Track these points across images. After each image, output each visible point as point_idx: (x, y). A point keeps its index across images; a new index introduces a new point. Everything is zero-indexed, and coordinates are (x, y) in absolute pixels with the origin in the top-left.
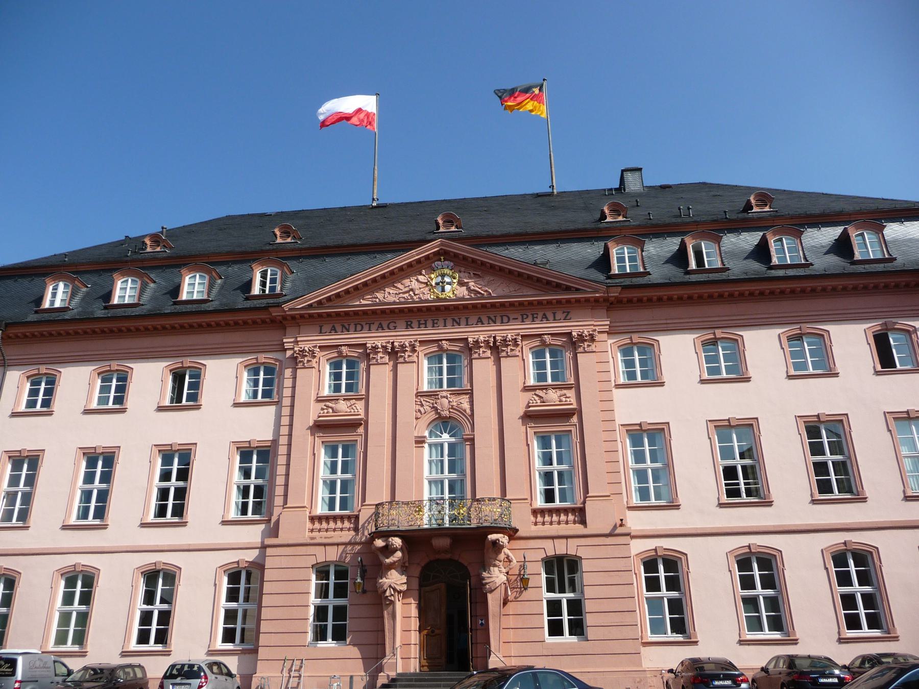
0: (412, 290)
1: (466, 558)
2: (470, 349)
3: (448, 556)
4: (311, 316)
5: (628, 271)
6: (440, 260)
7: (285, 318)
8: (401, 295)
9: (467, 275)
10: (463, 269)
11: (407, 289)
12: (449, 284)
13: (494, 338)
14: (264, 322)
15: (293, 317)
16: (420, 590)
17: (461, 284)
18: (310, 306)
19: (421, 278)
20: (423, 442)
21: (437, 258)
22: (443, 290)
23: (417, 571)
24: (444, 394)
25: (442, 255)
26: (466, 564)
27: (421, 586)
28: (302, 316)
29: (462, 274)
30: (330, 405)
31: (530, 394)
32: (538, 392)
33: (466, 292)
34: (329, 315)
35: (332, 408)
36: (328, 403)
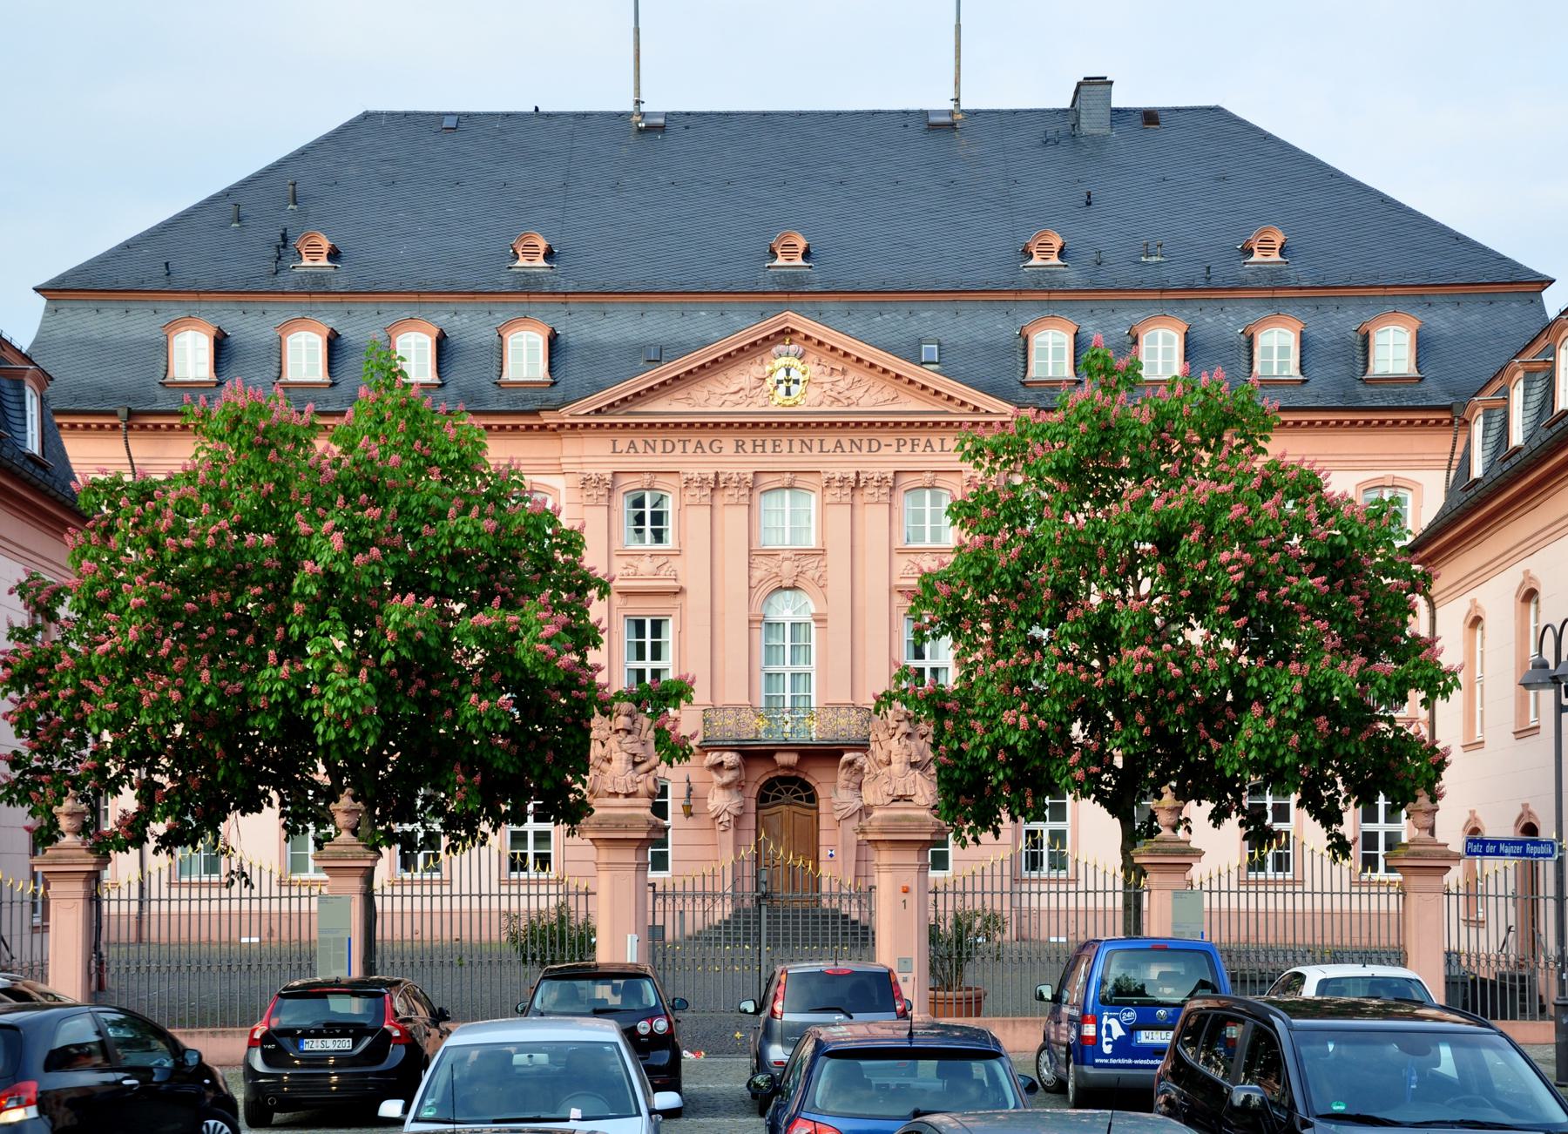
4: (600, 425)
12: (796, 382)
14: (529, 427)
15: (574, 426)
18: (598, 411)
22: (788, 393)
28: (587, 425)
34: (626, 425)
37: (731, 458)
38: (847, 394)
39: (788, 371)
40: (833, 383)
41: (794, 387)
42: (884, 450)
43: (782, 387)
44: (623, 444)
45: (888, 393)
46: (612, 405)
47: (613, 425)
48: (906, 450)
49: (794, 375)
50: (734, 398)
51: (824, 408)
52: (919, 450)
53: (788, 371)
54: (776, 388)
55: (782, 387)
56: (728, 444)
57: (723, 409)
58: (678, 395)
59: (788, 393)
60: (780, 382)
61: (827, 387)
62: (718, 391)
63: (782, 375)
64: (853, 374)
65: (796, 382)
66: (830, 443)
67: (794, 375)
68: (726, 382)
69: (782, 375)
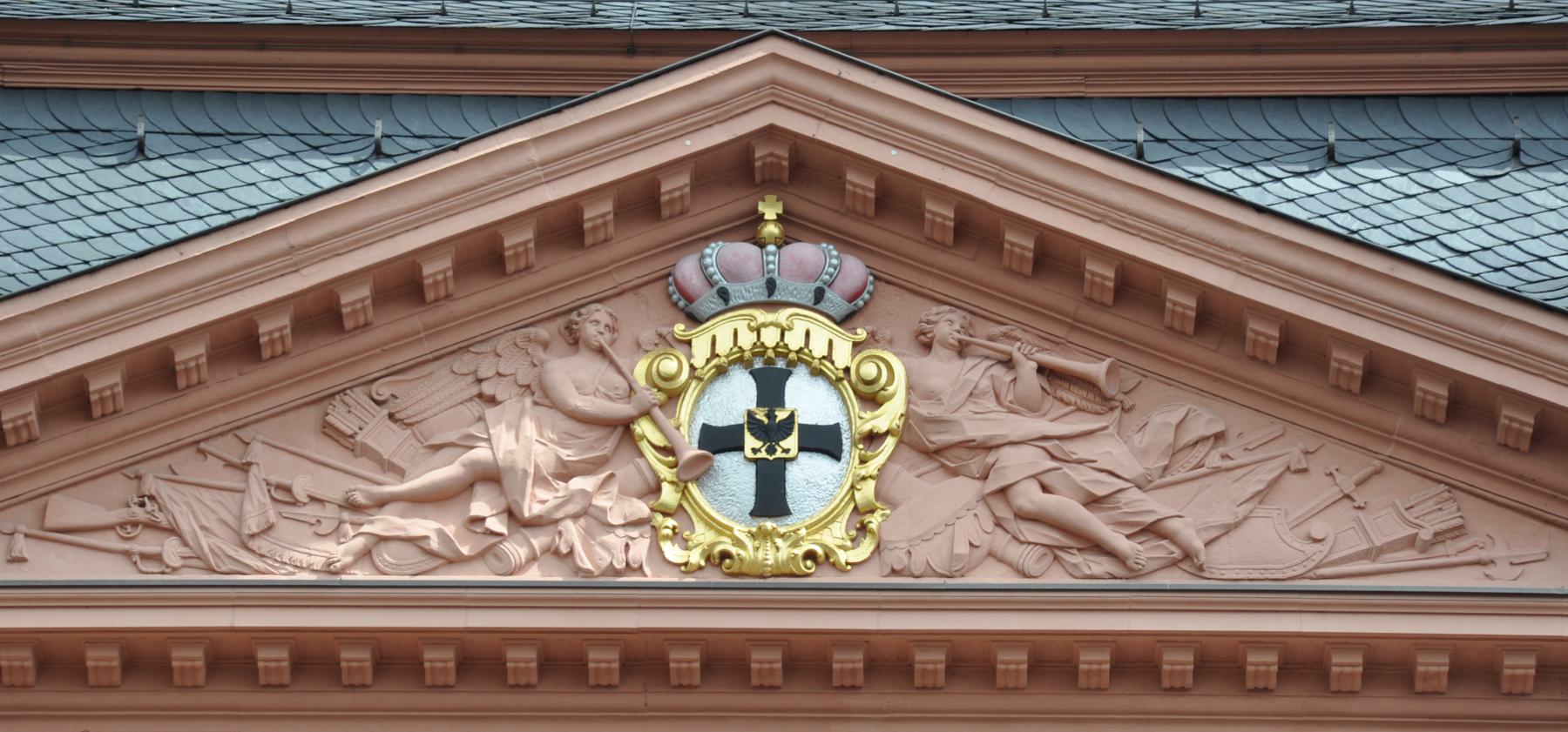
0: (490, 477)
6: (748, 227)
8: (386, 523)
9: (976, 372)
10: (948, 325)
11: (446, 471)
12: (823, 441)
17: (928, 445)
19: (578, 380)
21: (728, 204)
22: (771, 499)
25: (771, 184)
29: (942, 371)
33: (973, 528)
38: (1153, 506)
39: (771, 386)
41: (810, 477)
49: (809, 401)
53: (771, 386)
54: (695, 472)
55: (736, 475)
58: (69, 510)
59: (771, 499)
60: (720, 440)
61: (1017, 464)
62: (335, 487)
63: (736, 398)
64: (1169, 414)
65: (823, 441)
67: (809, 401)
68: (384, 438)
69: (736, 398)
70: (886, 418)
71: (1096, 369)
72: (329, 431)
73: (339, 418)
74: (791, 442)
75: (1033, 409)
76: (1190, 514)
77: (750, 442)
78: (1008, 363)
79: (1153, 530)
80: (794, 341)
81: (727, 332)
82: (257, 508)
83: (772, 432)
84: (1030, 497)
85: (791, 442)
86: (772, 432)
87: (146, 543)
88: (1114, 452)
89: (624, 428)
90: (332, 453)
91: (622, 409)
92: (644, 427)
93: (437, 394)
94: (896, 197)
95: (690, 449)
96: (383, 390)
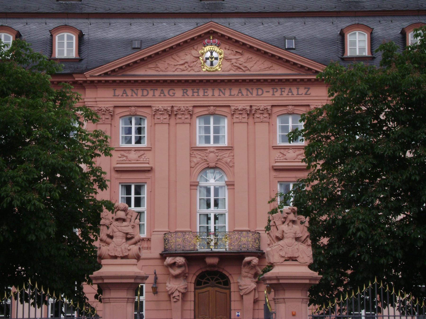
1: (229, 271)
2: (233, 115)
3: (216, 269)
4: (107, 81)
5: (358, 54)
7: (85, 82)
9: (229, 52)
13: (251, 106)
15: (92, 82)
16: (194, 292)
18: (106, 74)
19: (194, 52)
20: (197, 186)
22: (212, 64)
23: (192, 279)
24: (212, 150)
26: (227, 275)
27: (195, 289)
28: (100, 81)
29: (228, 52)
30: (126, 154)
31: (276, 154)
32: (282, 151)
33: (230, 67)
34: (121, 81)
35: (127, 157)
36: (122, 153)
37: (180, 99)
38: (245, 65)
40: (237, 59)
41: (215, 62)
42: (265, 94)
43: (209, 62)
44: (119, 92)
45: (267, 64)
46: (113, 71)
47: (114, 81)
48: (277, 94)
49: (215, 55)
50: (181, 67)
51: (232, 72)
52: (285, 94)
54: (205, 62)
55: (209, 62)
56: (179, 92)
57: (176, 73)
58: (151, 66)
59: (212, 64)
60: (207, 59)
61: (234, 61)
62: (173, 63)
63: (208, 55)
64: (247, 55)
65: (216, 59)
66: (235, 91)
67: (215, 55)
68: (177, 59)
69: (208, 55)
70: (222, 56)
71: (241, 52)
72: (172, 58)
73: (173, 57)
74: (213, 59)
75: (235, 55)
76: (249, 65)
77: (210, 59)
78: (233, 51)
79: (246, 67)
80: (214, 49)
81: (208, 48)
82: (166, 66)
83: (212, 58)
84: (235, 64)
85: (213, 59)
86: (212, 58)
87: (157, 69)
88: (242, 60)
89: (198, 58)
90: (172, 60)
91: (198, 56)
92: (200, 58)
93: (182, 54)
94: (223, 36)
95: (205, 59)
96: (177, 54)
